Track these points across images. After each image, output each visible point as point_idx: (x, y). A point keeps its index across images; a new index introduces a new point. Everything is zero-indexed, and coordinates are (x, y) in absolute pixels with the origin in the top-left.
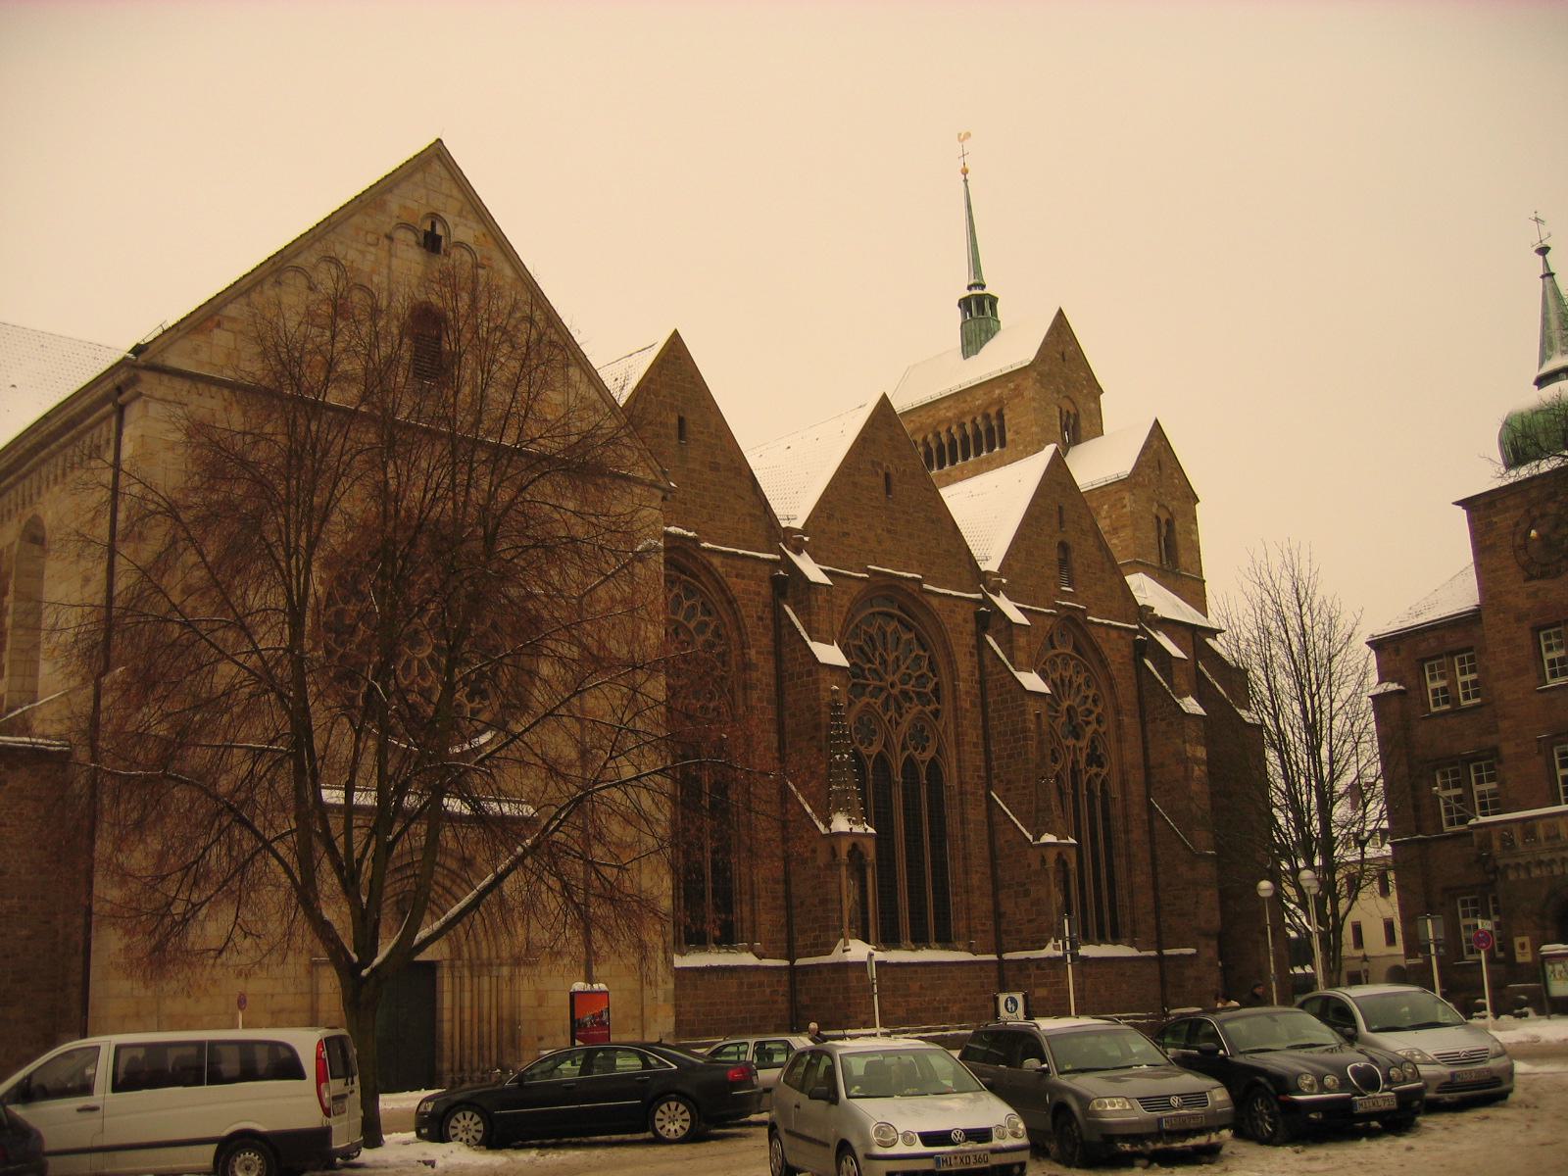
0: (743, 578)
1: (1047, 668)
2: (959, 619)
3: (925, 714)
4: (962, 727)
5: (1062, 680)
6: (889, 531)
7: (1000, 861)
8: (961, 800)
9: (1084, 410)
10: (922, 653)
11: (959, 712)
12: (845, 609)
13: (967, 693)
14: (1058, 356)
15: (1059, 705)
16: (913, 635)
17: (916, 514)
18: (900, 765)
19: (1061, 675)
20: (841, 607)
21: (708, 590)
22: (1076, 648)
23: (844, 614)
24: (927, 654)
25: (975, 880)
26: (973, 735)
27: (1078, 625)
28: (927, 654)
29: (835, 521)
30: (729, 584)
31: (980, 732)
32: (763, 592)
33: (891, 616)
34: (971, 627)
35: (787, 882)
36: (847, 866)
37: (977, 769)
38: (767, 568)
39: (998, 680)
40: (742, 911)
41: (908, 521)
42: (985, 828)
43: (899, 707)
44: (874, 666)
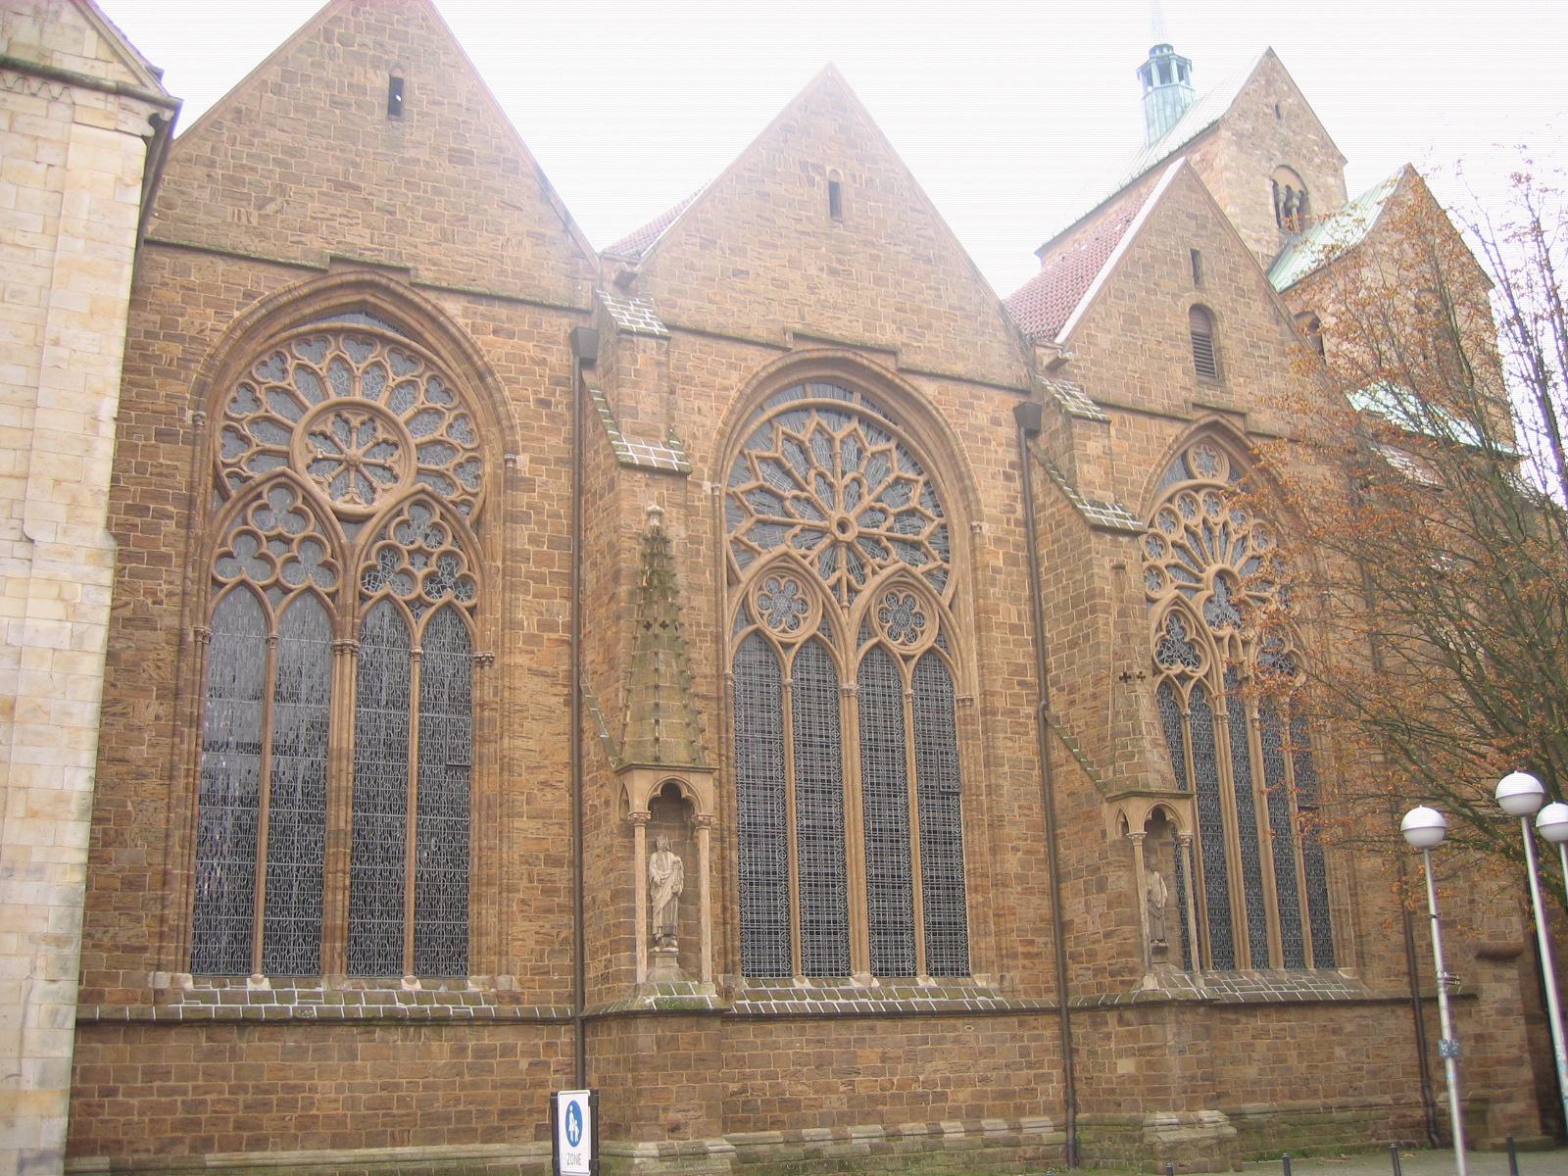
0: (511, 335)
1: (1176, 509)
2: (983, 419)
3: (914, 577)
4: (986, 597)
5: (1209, 530)
6: (833, 272)
7: (1065, 830)
8: (984, 723)
9: (1318, 188)
10: (911, 475)
11: (979, 572)
12: (734, 394)
13: (998, 541)
14: (1269, 111)
15: (1202, 571)
16: (892, 445)
17: (892, 248)
18: (855, 665)
19: (1205, 521)
20: (725, 389)
21: (438, 354)
22: (1235, 473)
24: (922, 479)
25: (1012, 863)
26: (1011, 611)
27: (1234, 439)
28: (922, 479)
29: (718, 252)
30: (479, 343)
31: (1026, 608)
32: (553, 359)
33: (847, 413)
34: (1008, 431)
35: (578, 864)
36: (648, 826)
37: (1019, 670)
38: (565, 321)
39: (1053, 514)
40: (484, 915)
41: (875, 258)
42: (1036, 772)
43: (858, 567)
44: (804, 495)
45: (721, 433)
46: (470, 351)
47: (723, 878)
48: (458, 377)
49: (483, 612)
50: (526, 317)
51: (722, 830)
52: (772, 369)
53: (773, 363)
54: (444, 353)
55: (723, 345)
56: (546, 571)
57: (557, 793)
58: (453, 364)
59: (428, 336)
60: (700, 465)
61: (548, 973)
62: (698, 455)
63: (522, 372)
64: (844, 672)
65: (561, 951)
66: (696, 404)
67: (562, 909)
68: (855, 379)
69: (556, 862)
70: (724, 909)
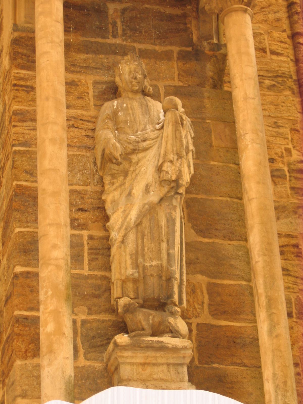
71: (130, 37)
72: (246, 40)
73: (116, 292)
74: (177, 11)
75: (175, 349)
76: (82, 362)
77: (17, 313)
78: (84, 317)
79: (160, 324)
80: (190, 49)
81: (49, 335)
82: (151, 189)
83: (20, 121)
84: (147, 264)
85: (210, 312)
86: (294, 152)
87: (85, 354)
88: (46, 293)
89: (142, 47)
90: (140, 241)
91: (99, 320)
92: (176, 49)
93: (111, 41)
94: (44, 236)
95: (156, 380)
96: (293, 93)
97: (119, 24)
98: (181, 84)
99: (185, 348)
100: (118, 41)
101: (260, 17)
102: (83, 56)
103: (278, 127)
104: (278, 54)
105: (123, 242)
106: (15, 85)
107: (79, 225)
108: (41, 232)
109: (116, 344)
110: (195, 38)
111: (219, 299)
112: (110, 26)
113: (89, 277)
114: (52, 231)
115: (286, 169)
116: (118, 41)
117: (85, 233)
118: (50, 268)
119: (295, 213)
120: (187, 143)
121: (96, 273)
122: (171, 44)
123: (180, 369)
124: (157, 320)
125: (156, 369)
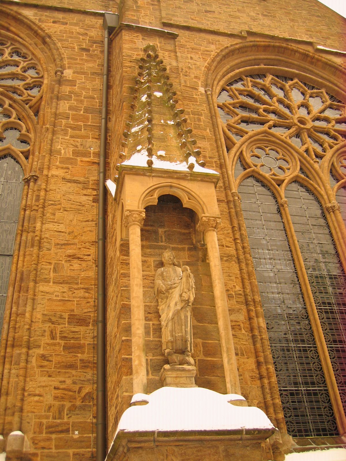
23: (212, 56)
30: (43, 26)
45: (208, 69)
46: (36, 28)
47: (253, 337)
48: (30, 44)
49: (33, 154)
50: (75, 18)
51: (246, 295)
52: (237, 46)
53: (237, 44)
54: (22, 35)
55: (203, 35)
56: (81, 124)
57: (84, 264)
58: (27, 39)
59: (12, 29)
60: (194, 80)
61: (67, 431)
62: (193, 76)
63: (71, 37)
64: (325, 197)
65: (83, 408)
66: (189, 56)
67: (85, 365)
68: (290, 61)
69: (82, 321)
70: (259, 364)
71: (168, 242)
72: (215, 242)
73: (164, 347)
74: (187, 231)
75: (189, 371)
76: (151, 376)
77: (123, 356)
78: (151, 358)
79: (183, 360)
80: (192, 246)
81: (136, 366)
82: (178, 304)
83: (123, 277)
84: (177, 335)
85: (204, 354)
86: (237, 287)
87: (152, 373)
88: (135, 348)
89: (173, 246)
90: (173, 325)
91: (157, 359)
92: (187, 246)
93: (161, 244)
94: (134, 324)
95: (181, 384)
96: (236, 263)
97: (163, 237)
98: (189, 260)
99: (193, 370)
100: (163, 244)
101: (221, 232)
102: (150, 250)
103: (230, 276)
104: (229, 247)
105: (166, 326)
106: (122, 263)
107: (148, 320)
108: (132, 322)
109: (164, 369)
110: (194, 242)
111: (207, 349)
112: (160, 238)
113: (152, 341)
114: (137, 323)
115: (234, 294)
116: (163, 244)
117: (151, 323)
118: (137, 337)
119: (238, 312)
120: (192, 284)
121: (156, 339)
122: (185, 245)
123: (191, 379)
124: (181, 358)
125: (181, 379)
